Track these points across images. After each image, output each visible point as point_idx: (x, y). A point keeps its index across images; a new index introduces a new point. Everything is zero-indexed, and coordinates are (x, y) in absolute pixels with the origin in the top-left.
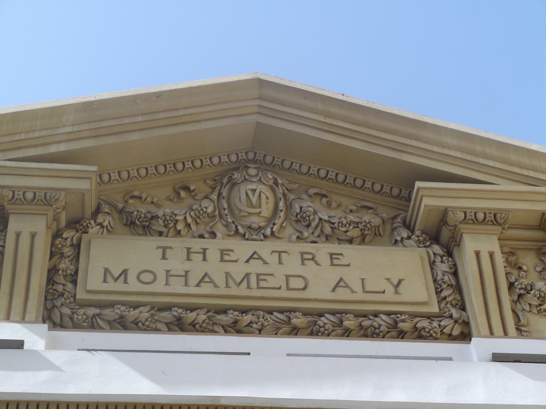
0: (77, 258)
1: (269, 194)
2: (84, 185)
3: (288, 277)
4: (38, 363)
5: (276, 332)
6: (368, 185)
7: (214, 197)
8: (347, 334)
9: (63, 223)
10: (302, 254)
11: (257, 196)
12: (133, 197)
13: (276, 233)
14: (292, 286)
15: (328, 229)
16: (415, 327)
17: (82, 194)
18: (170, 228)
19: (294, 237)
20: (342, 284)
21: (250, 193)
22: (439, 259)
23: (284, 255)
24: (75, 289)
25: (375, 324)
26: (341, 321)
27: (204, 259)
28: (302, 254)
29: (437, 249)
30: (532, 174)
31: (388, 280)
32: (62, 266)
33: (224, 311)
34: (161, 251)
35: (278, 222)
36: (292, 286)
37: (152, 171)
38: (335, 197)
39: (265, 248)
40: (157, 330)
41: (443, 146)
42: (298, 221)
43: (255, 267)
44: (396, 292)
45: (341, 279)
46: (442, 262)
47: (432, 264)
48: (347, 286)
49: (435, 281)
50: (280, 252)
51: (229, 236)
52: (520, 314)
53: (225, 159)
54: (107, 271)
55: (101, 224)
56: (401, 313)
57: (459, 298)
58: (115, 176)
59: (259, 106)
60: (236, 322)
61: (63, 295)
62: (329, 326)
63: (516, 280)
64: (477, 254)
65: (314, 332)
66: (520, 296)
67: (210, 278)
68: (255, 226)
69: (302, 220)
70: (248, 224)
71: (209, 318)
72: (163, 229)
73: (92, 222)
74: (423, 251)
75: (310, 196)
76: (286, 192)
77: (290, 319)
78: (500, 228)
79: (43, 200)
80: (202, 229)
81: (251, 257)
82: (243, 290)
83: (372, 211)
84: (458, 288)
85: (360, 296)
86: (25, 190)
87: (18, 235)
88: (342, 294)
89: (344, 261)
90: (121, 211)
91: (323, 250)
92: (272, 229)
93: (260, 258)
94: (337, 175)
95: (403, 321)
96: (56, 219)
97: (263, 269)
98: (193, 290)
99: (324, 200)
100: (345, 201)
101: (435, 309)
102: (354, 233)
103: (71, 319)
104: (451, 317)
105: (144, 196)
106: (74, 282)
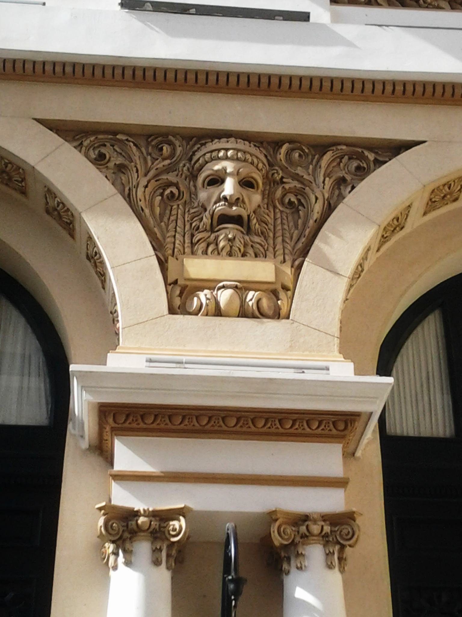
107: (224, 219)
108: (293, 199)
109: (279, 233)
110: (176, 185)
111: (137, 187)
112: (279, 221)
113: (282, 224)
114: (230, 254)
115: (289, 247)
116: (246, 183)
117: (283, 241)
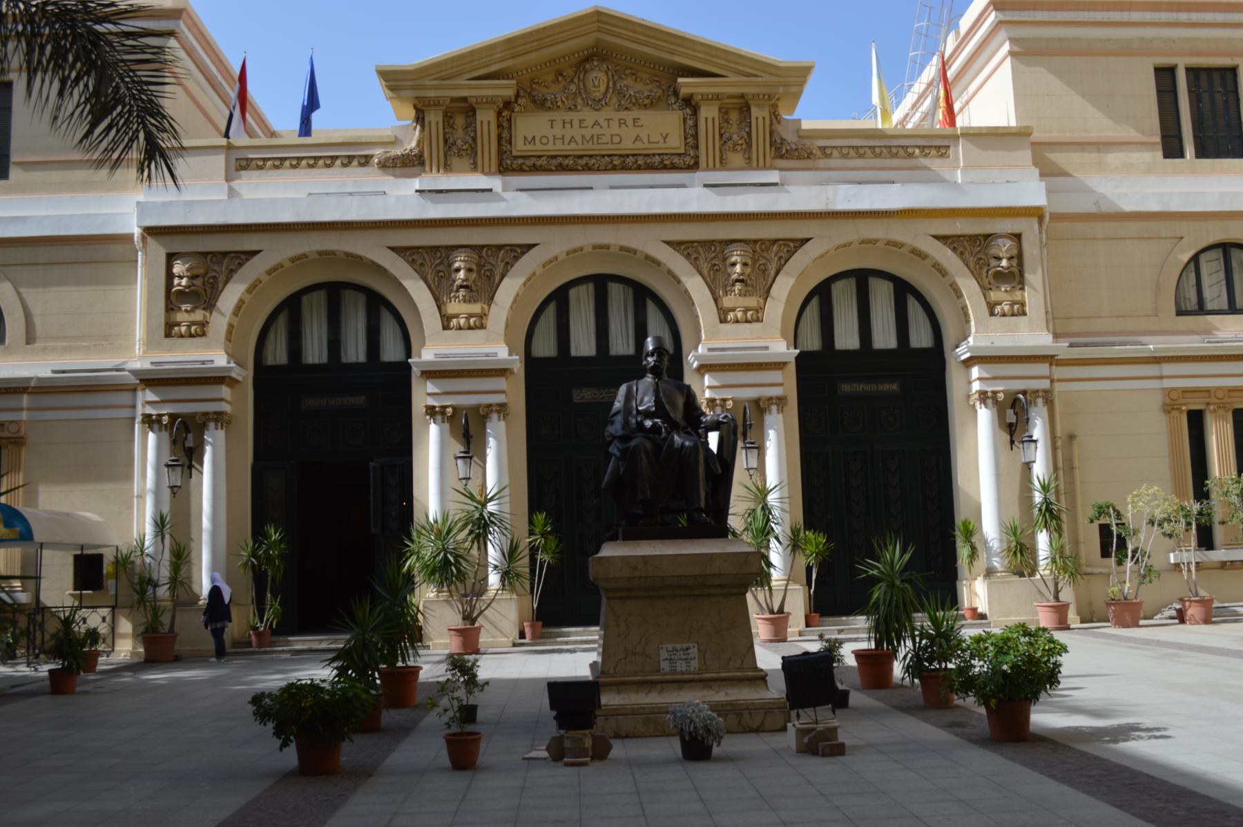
2: (510, 93)
8: (639, 168)
11: (598, 79)
18: (554, 107)
29: (688, 111)
30: (740, 68)
33: (581, 157)
38: (639, 74)
39: (601, 116)
40: (550, 170)
41: (694, 50)
43: (596, 130)
47: (685, 120)
65: (624, 168)
69: (620, 93)
79: (490, 101)
80: (569, 103)
82: (590, 146)
84: (696, 136)
85: (647, 145)
86: (482, 97)
88: (638, 145)
89: (640, 123)
91: (628, 116)
98: (567, 147)
100: (645, 76)
101: (682, 151)
102: (647, 102)
107: (461, 287)
116: (469, 270)
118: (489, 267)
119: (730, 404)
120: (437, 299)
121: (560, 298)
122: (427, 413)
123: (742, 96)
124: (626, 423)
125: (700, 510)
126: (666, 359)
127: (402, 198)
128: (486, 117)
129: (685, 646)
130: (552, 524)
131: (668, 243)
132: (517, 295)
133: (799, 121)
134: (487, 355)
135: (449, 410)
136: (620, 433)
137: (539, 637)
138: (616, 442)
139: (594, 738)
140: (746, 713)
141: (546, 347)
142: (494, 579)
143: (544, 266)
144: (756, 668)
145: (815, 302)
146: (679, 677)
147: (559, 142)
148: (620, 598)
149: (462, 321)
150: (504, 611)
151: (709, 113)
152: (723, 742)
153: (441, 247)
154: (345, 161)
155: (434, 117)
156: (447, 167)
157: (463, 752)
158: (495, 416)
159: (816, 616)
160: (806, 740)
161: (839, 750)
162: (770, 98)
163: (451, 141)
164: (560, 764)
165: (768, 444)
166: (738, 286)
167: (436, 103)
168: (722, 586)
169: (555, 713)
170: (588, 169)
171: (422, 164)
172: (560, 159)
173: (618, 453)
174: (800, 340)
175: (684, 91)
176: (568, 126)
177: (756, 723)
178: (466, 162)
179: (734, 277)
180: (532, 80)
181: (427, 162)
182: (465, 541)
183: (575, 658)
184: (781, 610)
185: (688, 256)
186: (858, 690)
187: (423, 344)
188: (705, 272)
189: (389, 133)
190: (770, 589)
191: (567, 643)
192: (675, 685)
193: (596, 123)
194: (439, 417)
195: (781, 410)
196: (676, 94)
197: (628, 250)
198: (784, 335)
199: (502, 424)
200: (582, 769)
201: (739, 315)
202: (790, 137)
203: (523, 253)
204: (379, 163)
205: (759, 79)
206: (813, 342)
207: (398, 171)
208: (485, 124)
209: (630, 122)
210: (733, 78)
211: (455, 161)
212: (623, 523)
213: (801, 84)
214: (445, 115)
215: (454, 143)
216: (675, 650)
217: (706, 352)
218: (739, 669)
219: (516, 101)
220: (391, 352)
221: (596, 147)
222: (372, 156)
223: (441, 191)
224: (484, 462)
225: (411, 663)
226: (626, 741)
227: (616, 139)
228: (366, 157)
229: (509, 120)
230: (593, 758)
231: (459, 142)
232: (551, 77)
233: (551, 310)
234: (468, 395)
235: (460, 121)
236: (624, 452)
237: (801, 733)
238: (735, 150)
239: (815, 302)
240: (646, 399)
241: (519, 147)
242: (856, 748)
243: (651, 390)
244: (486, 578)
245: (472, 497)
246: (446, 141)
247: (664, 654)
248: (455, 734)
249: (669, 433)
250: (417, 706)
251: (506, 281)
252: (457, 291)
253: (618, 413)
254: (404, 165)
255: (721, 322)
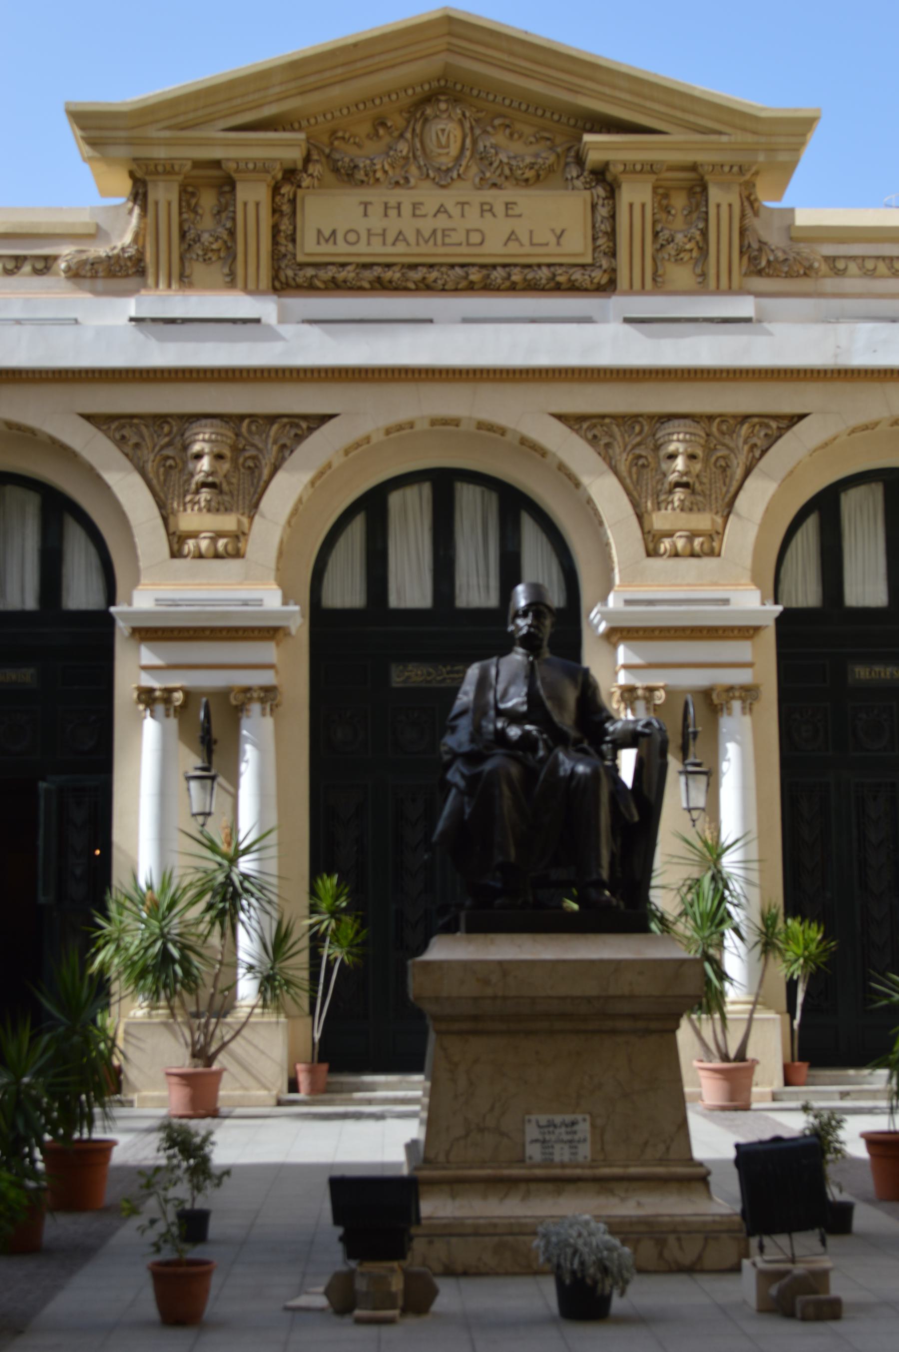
0: (294, 213)
1: (458, 133)
2: (295, 155)
3: (468, 232)
4: (272, 335)
5: (456, 290)
6: (548, 114)
7: (408, 135)
8: (513, 288)
9: (280, 176)
10: (482, 204)
11: (446, 132)
12: (337, 138)
13: (463, 176)
14: (472, 241)
15: (507, 171)
16: (569, 280)
17: (295, 162)
18: (370, 180)
19: (477, 180)
20: (513, 237)
21: (440, 133)
22: (600, 202)
23: (466, 207)
24: (295, 247)
25: (538, 277)
26: (509, 275)
27: (399, 215)
28: (482, 204)
29: (600, 191)
30: (692, 118)
31: (553, 231)
32: (283, 227)
33: (414, 267)
34: (362, 207)
35: (464, 163)
36: (472, 241)
37: (353, 109)
38: (518, 126)
39: (449, 198)
40: (361, 289)
41: (614, 87)
42: (481, 159)
43: (442, 222)
44: (558, 244)
45: (513, 233)
46: (603, 205)
47: (594, 207)
48: (517, 239)
49: (594, 227)
50: (463, 204)
51: (421, 180)
52: (659, 264)
53: (418, 89)
54: (319, 232)
55: (311, 175)
56: (561, 265)
57: (611, 244)
58: (321, 119)
59: (449, 43)
60: (424, 279)
61: (285, 256)
62: (499, 281)
63: (662, 230)
64: (631, 206)
65: (487, 288)
66: (662, 246)
67: (404, 236)
68: (444, 168)
69: (483, 159)
70: (437, 165)
71: (403, 275)
72: (365, 179)
73: (305, 175)
74: (588, 193)
75: (494, 127)
76: (474, 123)
77: (467, 274)
78: (654, 177)
79: (261, 168)
81: (438, 211)
83: (548, 143)
84: (612, 235)
85: (528, 249)
86: (247, 161)
87: (245, 204)
88: (513, 248)
89: (517, 211)
90: (328, 157)
91: (498, 198)
92: (458, 170)
93: (446, 211)
94: (520, 104)
95: (561, 275)
96: (274, 177)
97: (448, 224)
98: (390, 249)
99: (508, 131)
100: (528, 130)
101: (588, 260)
102: (529, 174)
103: (294, 279)
104: (601, 266)
105: (347, 136)
106: (294, 241)
107: (204, 485)
108: (250, 463)
109: (241, 492)
110: (173, 458)
111: (147, 461)
112: (241, 481)
113: (244, 483)
114: (209, 510)
115: (247, 502)
116: (219, 457)
117: (244, 498)
118: (251, 452)
119: (660, 697)
120: (162, 505)
121: (372, 507)
122: (140, 700)
123: (693, 167)
124: (477, 730)
125: (600, 885)
126: (548, 622)
127: (104, 331)
128: (253, 196)
129: (568, 1118)
130: (349, 896)
131: (560, 417)
132: (300, 501)
133: (791, 211)
134: (245, 603)
135: (178, 696)
136: (466, 748)
137: (322, 1091)
138: (459, 764)
139: (409, 1277)
140: (671, 1239)
141: (346, 591)
142: (247, 989)
143: (347, 452)
144: (690, 1160)
145: (811, 524)
146: (558, 1172)
147: (376, 241)
148: (460, 1033)
149: (204, 544)
150: (264, 1042)
151: (635, 195)
152: (630, 1289)
153: (171, 416)
154: (10, 265)
155: (164, 194)
156: (184, 280)
157: (180, 1295)
158: (256, 708)
159: (803, 1068)
160: (774, 1291)
161: (831, 1311)
162: (741, 170)
163: (191, 235)
164: (348, 1319)
165: (725, 766)
166: (679, 495)
167: (168, 170)
168: (634, 1017)
169: (340, 1231)
170: (426, 287)
171: (142, 272)
172: (377, 271)
173: (461, 783)
174: (785, 586)
175: (594, 157)
176: (393, 213)
177: (687, 1259)
178: (217, 271)
179: (673, 477)
180: (333, 133)
181: (151, 270)
182: (198, 922)
183: (380, 1131)
184: (741, 1056)
185: (593, 441)
186: (868, 1201)
187: (136, 582)
188: (623, 468)
189: (85, 218)
190: (723, 1018)
191: (370, 1102)
192: (550, 1186)
193: (441, 210)
194: (160, 708)
195: (748, 709)
196: (580, 161)
197: (490, 428)
198: (756, 580)
199: (269, 722)
200: (386, 1331)
201: (680, 543)
202: (775, 239)
203: (311, 430)
204: (68, 269)
205: (724, 139)
206: (806, 593)
207: (100, 284)
208: (251, 209)
209: (499, 209)
210: (678, 136)
211: (198, 270)
212: (468, 902)
213: (796, 148)
214: (183, 190)
215: (197, 240)
216: (552, 1124)
217: (621, 606)
218: (661, 1161)
219: (305, 169)
220: (81, 594)
221: (441, 250)
222: (55, 258)
223: (172, 321)
224: (236, 784)
225: (97, 1135)
226: (464, 1282)
227: (475, 238)
228: (46, 258)
229: (293, 201)
230: (405, 1311)
231: (206, 237)
232: (365, 129)
233: (357, 528)
234: (211, 671)
235: (208, 200)
236: (472, 781)
237: (766, 1277)
238: (678, 260)
239: (811, 524)
240: (512, 690)
241: (309, 247)
242: (862, 1308)
243: (522, 674)
244: (232, 987)
245: (212, 847)
246: (183, 235)
247: (532, 1132)
248: (167, 1264)
249: (550, 750)
250: (107, 1210)
251: (280, 476)
252: (197, 492)
253: (463, 713)
254: (111, 274)
255: (649, 555)
